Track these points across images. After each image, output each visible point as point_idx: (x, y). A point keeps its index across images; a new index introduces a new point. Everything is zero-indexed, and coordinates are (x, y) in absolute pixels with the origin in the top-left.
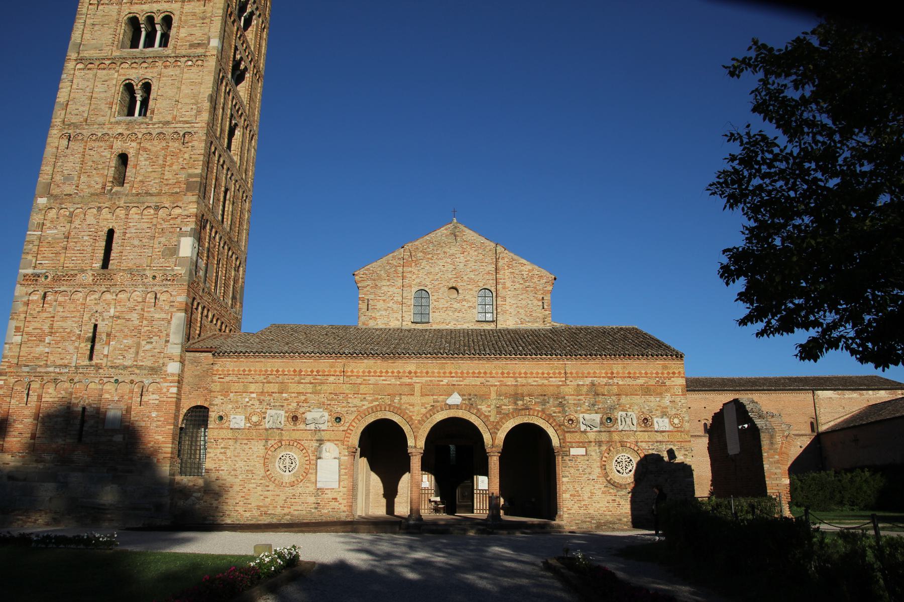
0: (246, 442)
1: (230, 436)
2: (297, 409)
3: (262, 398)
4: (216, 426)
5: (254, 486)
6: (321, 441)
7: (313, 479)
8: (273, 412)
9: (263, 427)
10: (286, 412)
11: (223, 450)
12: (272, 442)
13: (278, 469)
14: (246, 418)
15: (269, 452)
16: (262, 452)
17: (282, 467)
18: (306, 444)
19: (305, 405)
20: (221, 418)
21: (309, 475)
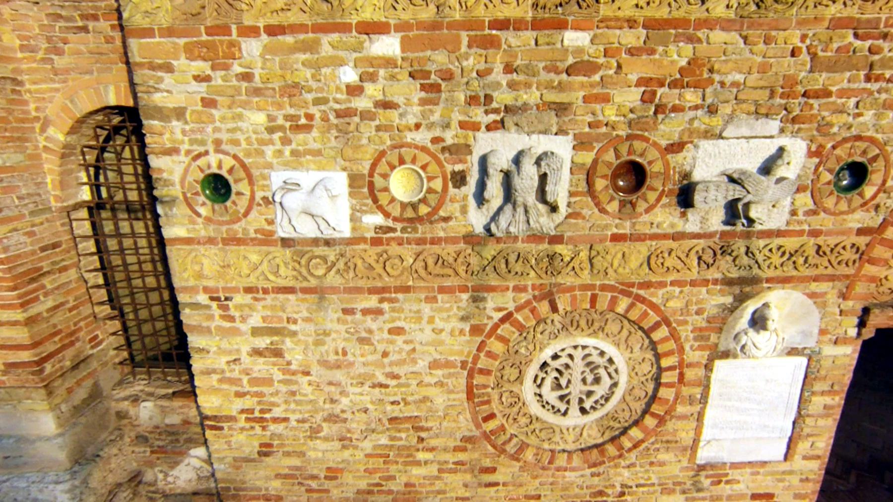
0: (372, 302)
1: (286, 276)
2: (638, 128)
3: (440, 59)
4: (202, 231)
5: (433, 470)
6: (744, 287)
7: (686, 437)
8: (501, 147)
9: (456, 227)
10: (581, 144)
11: (263, 342)
12: (508, 300)
13: (535, 408)
14: (354, 180)
15: (496, 346)
16: (460, 346)
17: (551, 396)
18: (674, 301)
19: (691, 97)
20: (218, 187)
21: (670, 425)
